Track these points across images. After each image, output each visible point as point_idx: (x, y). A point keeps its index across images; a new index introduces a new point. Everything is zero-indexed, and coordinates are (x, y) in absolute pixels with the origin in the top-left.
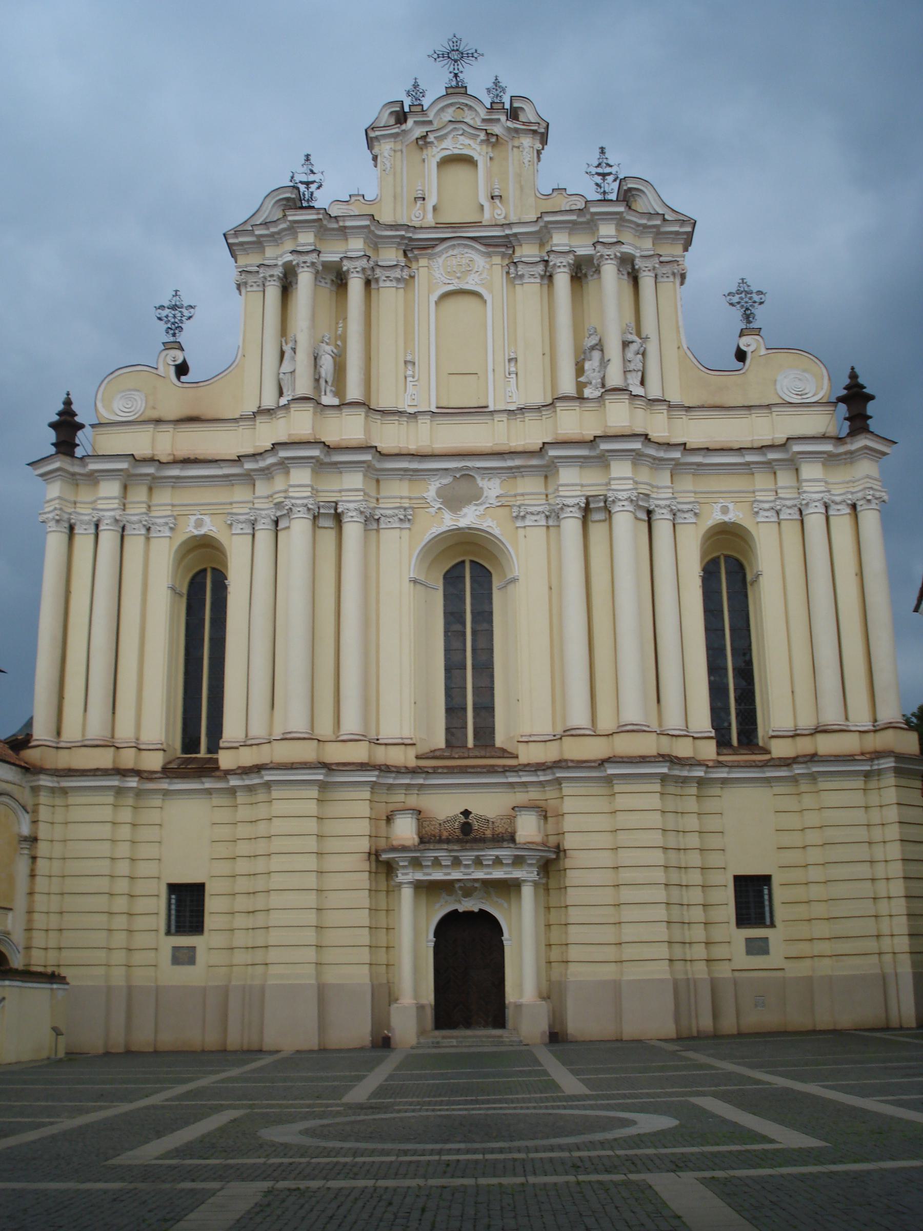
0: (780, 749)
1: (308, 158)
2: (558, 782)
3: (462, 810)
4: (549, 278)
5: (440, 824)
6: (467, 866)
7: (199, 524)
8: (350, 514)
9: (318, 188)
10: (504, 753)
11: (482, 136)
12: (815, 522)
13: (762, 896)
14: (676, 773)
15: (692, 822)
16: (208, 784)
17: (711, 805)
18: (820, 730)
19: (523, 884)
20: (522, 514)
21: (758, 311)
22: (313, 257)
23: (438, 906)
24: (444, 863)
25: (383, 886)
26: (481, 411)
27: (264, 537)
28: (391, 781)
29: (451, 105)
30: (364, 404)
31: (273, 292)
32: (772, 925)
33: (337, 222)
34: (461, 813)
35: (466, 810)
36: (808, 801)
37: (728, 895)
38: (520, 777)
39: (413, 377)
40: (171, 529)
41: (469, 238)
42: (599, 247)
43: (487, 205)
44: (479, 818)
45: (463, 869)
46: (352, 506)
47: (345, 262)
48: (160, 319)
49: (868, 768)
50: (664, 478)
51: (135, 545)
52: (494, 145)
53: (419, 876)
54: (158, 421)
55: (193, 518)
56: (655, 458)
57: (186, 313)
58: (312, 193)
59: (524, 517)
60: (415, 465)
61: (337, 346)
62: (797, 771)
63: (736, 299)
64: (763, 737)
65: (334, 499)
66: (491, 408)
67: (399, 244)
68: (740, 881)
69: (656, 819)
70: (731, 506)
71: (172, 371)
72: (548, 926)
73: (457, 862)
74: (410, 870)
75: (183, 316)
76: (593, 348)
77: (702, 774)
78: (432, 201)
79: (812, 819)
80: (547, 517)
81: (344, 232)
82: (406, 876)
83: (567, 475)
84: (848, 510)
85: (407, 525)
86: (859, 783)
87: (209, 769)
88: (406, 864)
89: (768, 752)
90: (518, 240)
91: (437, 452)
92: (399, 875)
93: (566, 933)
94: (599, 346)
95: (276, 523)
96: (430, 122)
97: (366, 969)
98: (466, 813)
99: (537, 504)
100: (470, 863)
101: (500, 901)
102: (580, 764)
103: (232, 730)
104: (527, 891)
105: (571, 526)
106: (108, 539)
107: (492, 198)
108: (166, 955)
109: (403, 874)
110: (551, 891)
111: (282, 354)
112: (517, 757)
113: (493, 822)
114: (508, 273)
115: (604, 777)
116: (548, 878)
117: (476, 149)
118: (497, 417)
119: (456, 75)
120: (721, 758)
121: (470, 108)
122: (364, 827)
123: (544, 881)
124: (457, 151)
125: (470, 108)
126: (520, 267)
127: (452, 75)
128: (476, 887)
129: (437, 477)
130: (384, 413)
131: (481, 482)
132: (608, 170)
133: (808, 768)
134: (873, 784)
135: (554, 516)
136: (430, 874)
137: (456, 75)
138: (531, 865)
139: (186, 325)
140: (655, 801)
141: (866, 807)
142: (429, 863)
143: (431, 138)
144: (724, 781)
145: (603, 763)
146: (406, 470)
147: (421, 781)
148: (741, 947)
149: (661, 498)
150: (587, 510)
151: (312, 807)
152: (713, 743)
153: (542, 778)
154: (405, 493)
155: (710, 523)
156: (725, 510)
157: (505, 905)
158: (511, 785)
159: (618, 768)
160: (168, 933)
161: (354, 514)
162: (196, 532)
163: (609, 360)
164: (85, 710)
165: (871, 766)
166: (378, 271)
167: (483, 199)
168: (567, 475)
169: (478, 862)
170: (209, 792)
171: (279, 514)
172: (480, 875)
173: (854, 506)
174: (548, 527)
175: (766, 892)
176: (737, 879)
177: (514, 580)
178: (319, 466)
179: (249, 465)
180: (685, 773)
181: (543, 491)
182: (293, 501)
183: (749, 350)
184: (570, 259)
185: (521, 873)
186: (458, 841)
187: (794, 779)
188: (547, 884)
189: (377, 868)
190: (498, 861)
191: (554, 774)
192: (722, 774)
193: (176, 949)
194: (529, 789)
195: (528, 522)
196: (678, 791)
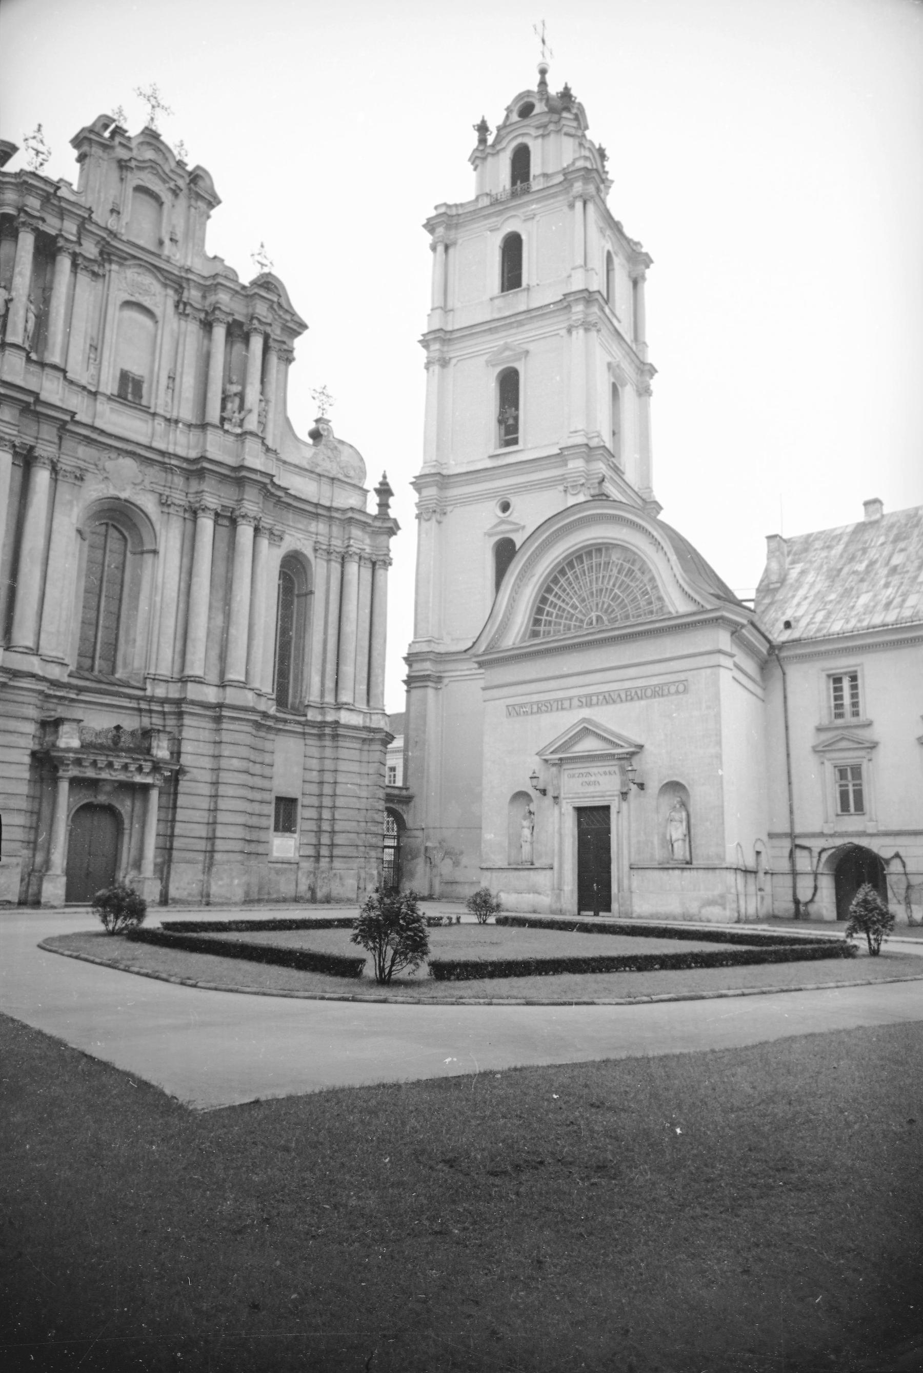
1: (40, 126)
8: (42, 460)
20: (169, 502)
33: (60, 202)
36: (328, 752)
37: (271, 809)
39: (95, 360)
42: (255, 322)
56: (268, 491)
59: (169, 506)
60: (94, 436)
65: (32, 444)
66: (152, 411)
67: (98, 243)
68: (279, 799)
76: (235, 395)
80: (185, 510)
81: (62, 214)
89: (305, 715)
90: (188, 284)
94: (241, 396)
104: (154, 794)
105: (206, 524)
114: (177, 307)
119: (152, 119)
120: (278, 715)
126: (188, 308)
127: (149, 118)
129: (106, 452)
135: (193, 512)
137: (152, 119)
145: (220, 706)
150: (217, 515)
161: (47, 462)
174: (185, 519)
183: (325, 433)
184: (230, 319)
186: (109, 749)
196: (254, 732)
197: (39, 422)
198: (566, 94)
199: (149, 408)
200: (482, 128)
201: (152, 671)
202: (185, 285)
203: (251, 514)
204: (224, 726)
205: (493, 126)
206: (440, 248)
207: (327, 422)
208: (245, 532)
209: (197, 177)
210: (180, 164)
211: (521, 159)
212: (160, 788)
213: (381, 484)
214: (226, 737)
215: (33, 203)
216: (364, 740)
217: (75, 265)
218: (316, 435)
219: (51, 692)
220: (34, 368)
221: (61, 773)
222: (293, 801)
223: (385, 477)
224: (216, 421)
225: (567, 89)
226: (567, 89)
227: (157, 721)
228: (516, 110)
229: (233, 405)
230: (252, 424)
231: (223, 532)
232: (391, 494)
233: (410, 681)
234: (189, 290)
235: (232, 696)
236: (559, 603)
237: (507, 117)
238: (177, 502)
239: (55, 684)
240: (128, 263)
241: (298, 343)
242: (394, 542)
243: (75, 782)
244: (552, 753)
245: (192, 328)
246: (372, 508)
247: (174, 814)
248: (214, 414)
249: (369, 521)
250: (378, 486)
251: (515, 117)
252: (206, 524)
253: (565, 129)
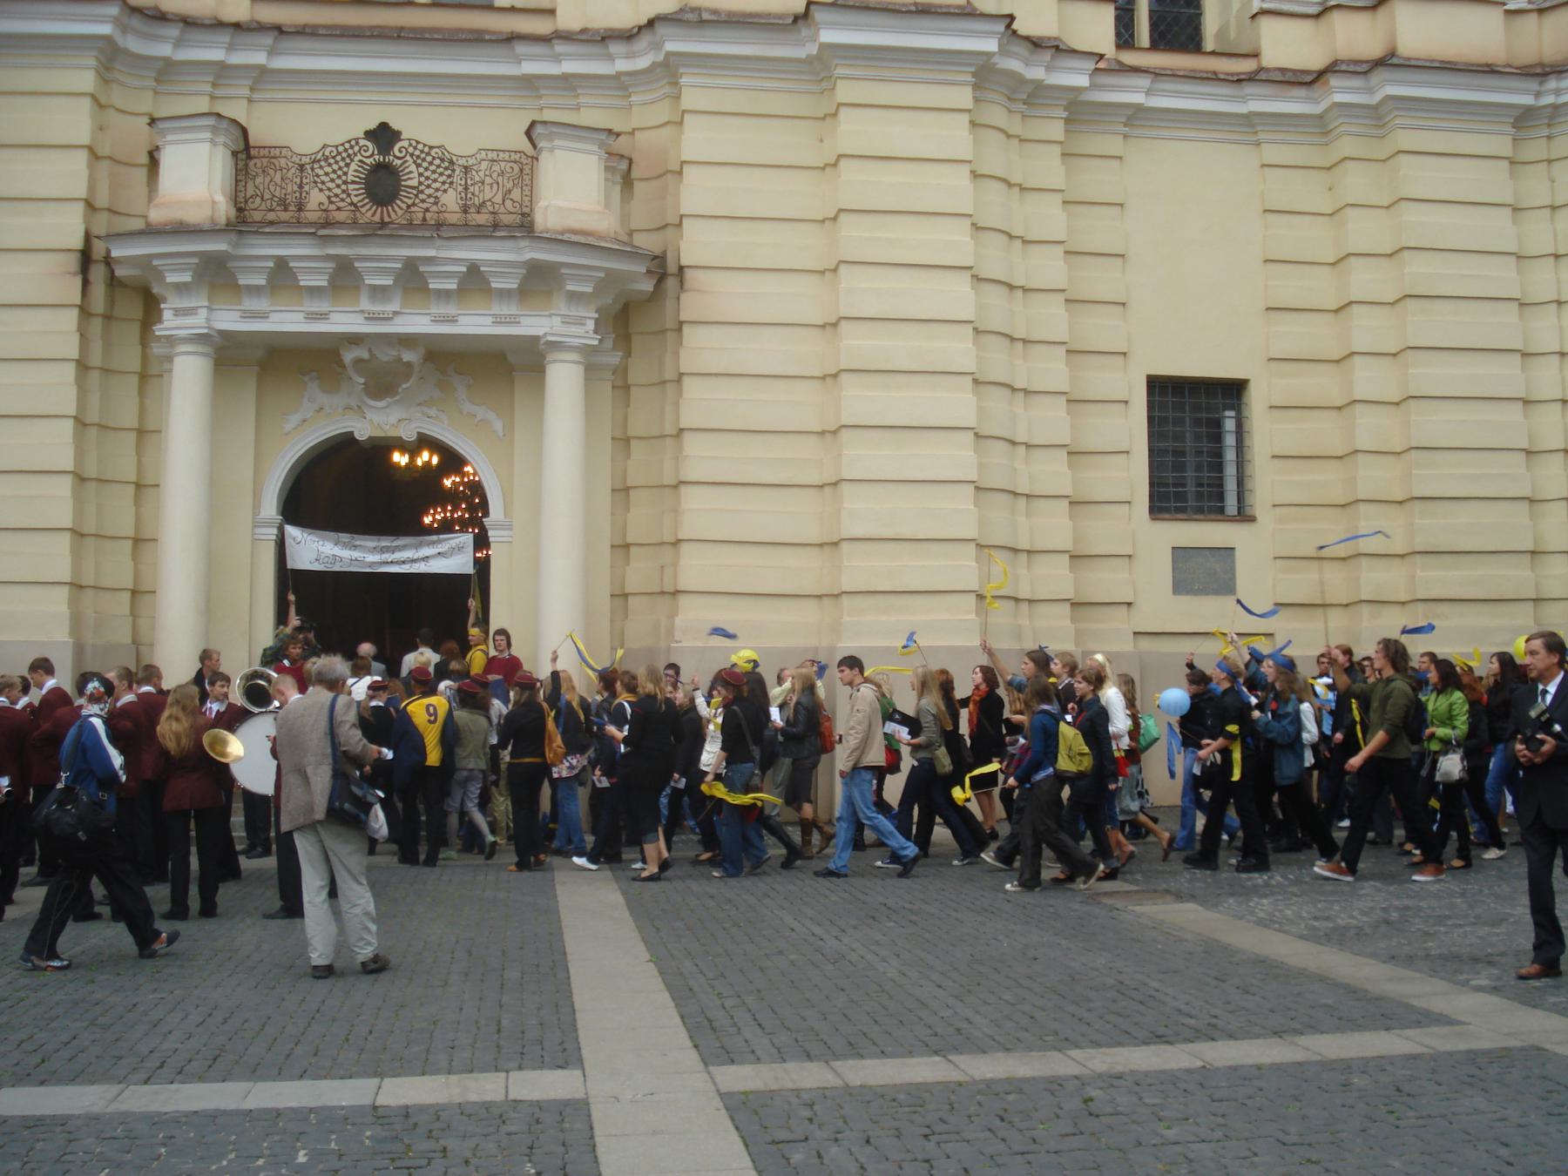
3: (372, 125)
5: (302, 167)
6: (378, 292)
13: (1218, 437)
14: (1014, 65)
15: (1048, 218)
17: (1097, 180)
19: (550, 357)
24: (306, 281)
25: (129, 358)
28: (165, 50)
32: (1244, 516)
34: (369, 135)
35: (384, 126)
36: (1357, 183)
38: (557, 59)
44: (423, 153)
45: (365, 304)
49: (1528, 100)
53: (229, 320)
62: (1339, 98)
64: (1221, 33)
69: (954, 188)
72: (622, 492)
73: (344, 278)
74: (199, 300)
77: (1082, 81)
79: (1366, 231)
86: (1501, 144)
88: (186, 277)
92: (167, 315)
93: (676, 511)
97: (58, 602)
98: (384, 136)
100: (388, 281)
101: (481, 412)
109: (178, 312)
110: (633, 390)
113: (467, 169)
115: (809, 60)
116: (628, 354)
122: (71, 174)
123: (615, 359)
128: (409, 365)
133: (1370, 91)
134: (1535, 149)
136: (263, 316)
138: (575, 297)
140: (954, 137)
141: (1516, 210)
142: (261, 281)
144: (1136, 116)
147: (259, 58)
153: (622, 65)
157: (498, 426)
158: (530, 83)
159: (857, 27)
165: (1538, 95)
169: (412, 280)
172: (418, 322)
175: (1230, 425)
176: (1159, 387)
180: (1036, 73)
185: (544, 321)
187: (1320, 126)
188: (621, 371)
189: (111, 301)
190: (474, 282)
191: (657, 46)
192: (1132, 93)
194: (582, 100)
196: (1015, 127)
212: (587, 351)
216: (1523, 119)
221: (170, 323)
222: (1232, 391)
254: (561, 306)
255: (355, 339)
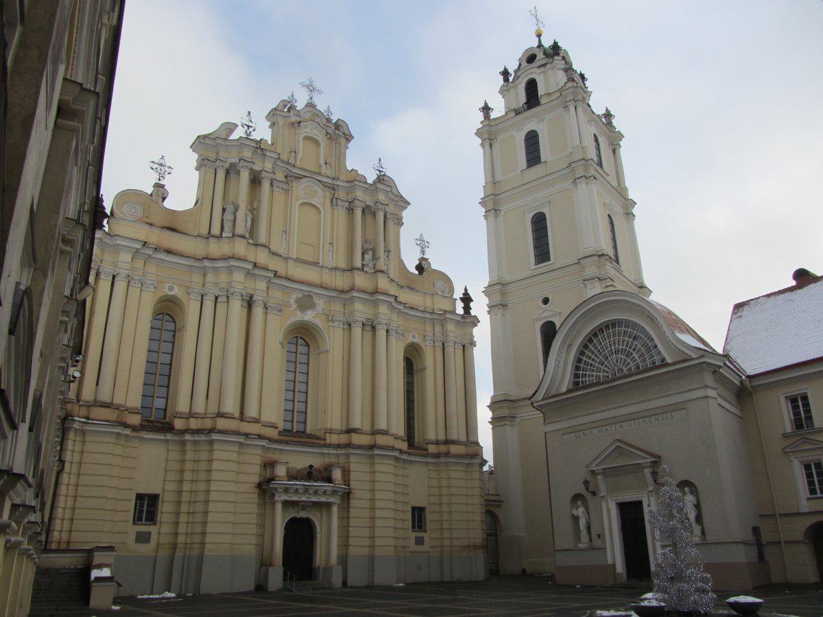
0: (432, 449)
1: (249, 112)
2: (348, 455)
4: (351, 210)
6: (310, 494)
7: (171, 289)
9: (254, 130)
10: (315, 437)
11: (325, 133)
12: (450, 348)
16: (169, 436)
18: (447, 442)
21: (427, 250)
22: (250, 165)
23: (287, 514)
26: (316, 264)
27: (208, 305)
29: (309, 112)
30: (265, 246)
31: (221, 175)
32: (425, 531)
37: (409, 516)
40: (155, 287)
41: (318, 180)
43: (324, 166)
45: (307, 496)
46: (260, 298)
47: (263, 173)
48: (152, 168)
50: (394, 317)
51: (135, 292)
52: (329, 139)
53: (285, 497)
54: (151, 225)
55: (167, 285)
56: (393, 307)
57: (168, 170)
58: (250, 132)
61: (252, 213)
63: (419, 242)
66: (321, 265)
68: (414, 509)
70: (416, 335)
71: (161, 199)
75: (165, 171)
78: (300, 156)
82: (281, 497)
83: (358, 306)
84: (462, 347)
85: (280, 314)
87: (167, 427)
89: (427, 450)
91: (296, 280)
92: (276, 497)
94: (374, 251)
95: (216, 298)
96: (300, 116)
99: (340, 317)
102: (360, 447)
103: (183, 406)
104: (335, 509)
105: (357, 331)
106: (120, 286)
107: (326, 164)
108: (133, 537)
111: (224, 210)
112: (325, 440)
114: (332, 202)
117: (321, 138)
118: (324, 270)
119: (311, 98)
120: (410, 451)
121: (318, 117)
122: (257, 469)
124: (311, 135)
125: (318, 117)
126: (339, 201)
130: (274, 254)
131: (314, 298)
132: (381, 169)
137: (311, 98)
138: (338, 495)
139: (167, 176)
140: (391, 469)
143: (302, 124)
144: (411, 461)
146: (283, 285)
148: (413, 540)
149: (393, 326)
150: (363, 324)
151: (233, 456)
152: (406, 443)
153: (339, 452)
154: (281, 298)
155: (408, 341)
156: (414, 337)
157: (319, 515)
158: (323, 453)
160: (134, 523)
162: (169, 293)
163: (379, 258)
164: (97, 384)
166: (275, 181)
167: (322, 163)
168: (358, 306)
170: (167, 441)
171: (220, 293)
172: (314, 499)
173: (464, 346)
177: (327, 351)
178: (248, 273)
179: (207, 263)
181: (343, 310)
182: (236, 290)
187: (437, 464)
192: (412, 458)
193: (138, 533)
195: (336, 324)
197: (255, 280)
198: (556, 48)
199: (319, 263)
200: (505, 73)
201: (329, 427)
202: (336, 189)
203: (384, 322)
204: (376, 461)
205: (511, 71)
206: (487, 146)
207: (426, 260)
208: (381, 334)
209: (338, 125)
210: (329, 120)
211: (531, 87)
213: (464, 294)
214: (378, 468)
215: (247, 154)
216: (467, 465)
217: (272, 185)
218: (420, 268)
219: (268, 446)
220: (251, 247)
221: (277, 498)
223: (466, 290)
224: (359, 265)
225: (555, 43)
226: (555, 43)
227: (333, 460)
228: (525, 59)
229: (368, 256)
230: (381, 265)
231: (368, 335)
232: (472, 300)
233: (495, 421)
234: (338, 191)
235: (381, 440)
236: (590, 362)
237: (520, 65)
238: (338, 318)
239: (271, 440)
240: (302, 180)
241: (405, 214)
242: (476, 331)
243: (286, 504)
244: (596, 466)
245: (341, 213)
246: (460, 310)
247: (348, 522)
248: (358, 263)
249: (459, 319)
250: (462, 296)
251: (524, 64)
252: (357, 331)
253: (557, 66)
254: (337, 497)
255: (303, 501)
